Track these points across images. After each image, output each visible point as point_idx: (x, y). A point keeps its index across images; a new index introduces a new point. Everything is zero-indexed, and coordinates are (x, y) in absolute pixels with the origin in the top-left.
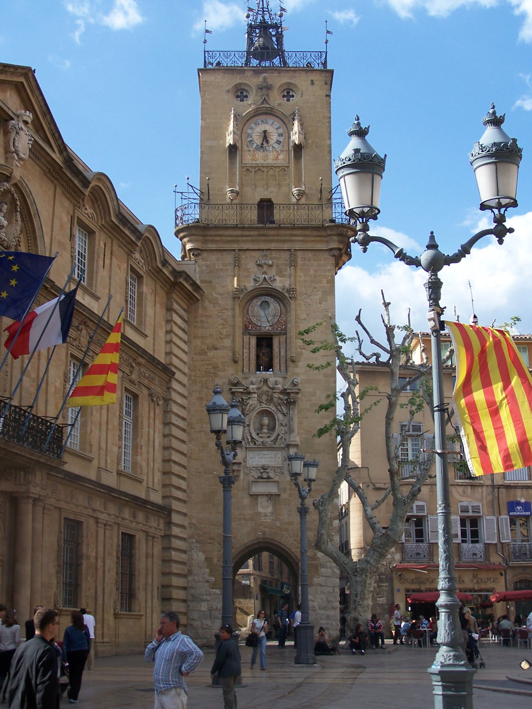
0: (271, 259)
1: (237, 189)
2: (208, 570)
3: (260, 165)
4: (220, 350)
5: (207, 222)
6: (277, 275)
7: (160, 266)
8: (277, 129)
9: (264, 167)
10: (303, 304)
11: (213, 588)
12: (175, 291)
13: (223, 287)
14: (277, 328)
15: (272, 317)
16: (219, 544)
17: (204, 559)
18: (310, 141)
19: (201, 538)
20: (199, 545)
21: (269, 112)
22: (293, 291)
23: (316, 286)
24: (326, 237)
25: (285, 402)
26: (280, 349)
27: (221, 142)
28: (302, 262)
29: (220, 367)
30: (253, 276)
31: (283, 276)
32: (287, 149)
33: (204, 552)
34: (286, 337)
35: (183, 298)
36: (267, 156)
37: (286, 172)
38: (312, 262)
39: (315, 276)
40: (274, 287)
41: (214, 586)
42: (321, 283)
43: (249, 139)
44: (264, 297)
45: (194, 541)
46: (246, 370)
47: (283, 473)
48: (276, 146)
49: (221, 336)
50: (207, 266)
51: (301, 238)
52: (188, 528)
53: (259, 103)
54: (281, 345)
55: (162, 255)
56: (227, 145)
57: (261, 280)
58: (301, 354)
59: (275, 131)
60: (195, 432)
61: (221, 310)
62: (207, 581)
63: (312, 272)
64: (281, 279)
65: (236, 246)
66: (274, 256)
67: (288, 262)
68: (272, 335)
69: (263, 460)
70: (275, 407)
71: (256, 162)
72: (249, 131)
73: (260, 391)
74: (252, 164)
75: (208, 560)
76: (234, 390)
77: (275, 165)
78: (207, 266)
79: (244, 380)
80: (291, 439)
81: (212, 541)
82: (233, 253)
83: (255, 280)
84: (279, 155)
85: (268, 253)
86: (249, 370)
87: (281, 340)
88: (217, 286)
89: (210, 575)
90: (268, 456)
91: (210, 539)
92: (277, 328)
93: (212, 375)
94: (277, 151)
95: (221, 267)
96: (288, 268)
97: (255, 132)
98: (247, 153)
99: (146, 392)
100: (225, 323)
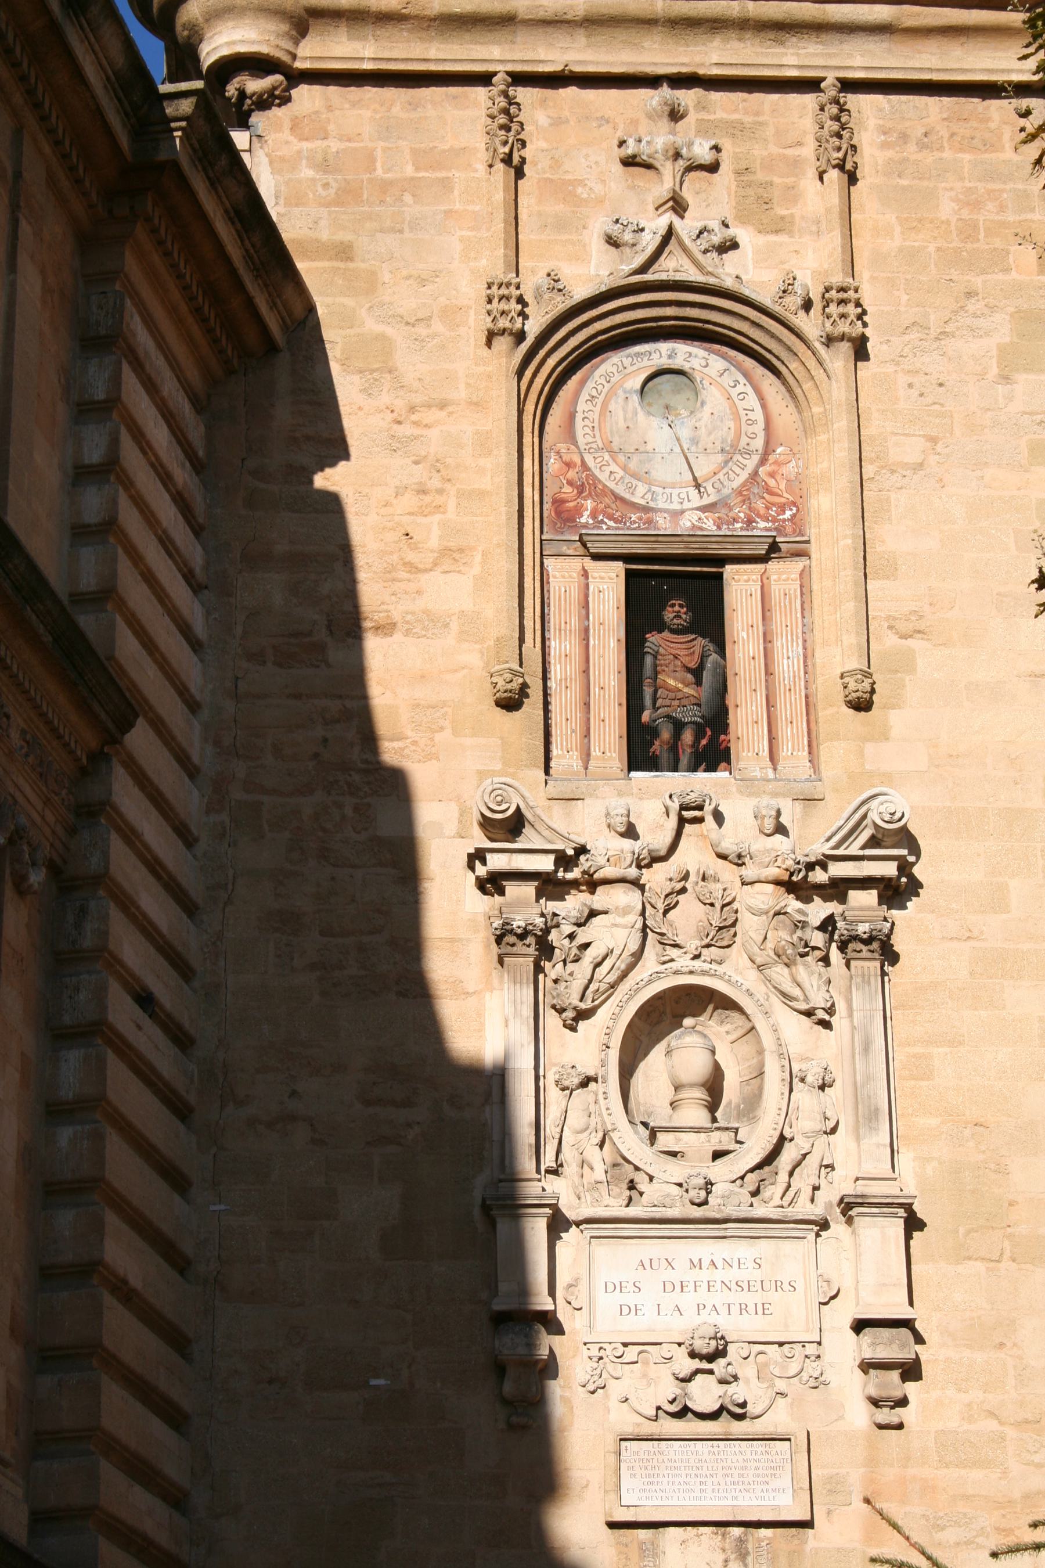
4: (407, 633)
6: (744, 219)
10: (902, 380)
13: (423, 282)
14: (750, 522)
15: (720, 458)
22: (842, 302)
23: (978, 282)
25: (818, 939)
26: (767, 639)
28: (890, 153)
29: (409, 733)
30: (600, 224)
31: (780, 227)
34: (805, 575)
35: (184, 308)
38: (947, 154)
39: (969, 231)
40: (729, 283)
42: (1007, 270)
44: (665, 347)
46: (564, 758)
47: (818, 1383)
49: (411, 556)
50: (325, 165)
54: (778, 618)
57: (649, 242)
58: (906, 663)
61: (412, 409)
63: (946, 209)
64: (762, 240)
66: (720, 115)
67: (808, 150)
68: (722, 561)
69: (688, 1300)
70: (753, 974)
73: (657, 877)
76: (497, 862)
78: (325, 165)
79: (557, 807)
80: (869, 1168)
82: (480, 93)
83: (613, 242)
85: (687, 97)
86: (586, 756)
87: (776, 589)
88: (387, 277)
90: (718, 1275)
92: (750, 522)
93: (356, 778)
95: (409, 171)
96: (809, 182)
100: (435, 483)
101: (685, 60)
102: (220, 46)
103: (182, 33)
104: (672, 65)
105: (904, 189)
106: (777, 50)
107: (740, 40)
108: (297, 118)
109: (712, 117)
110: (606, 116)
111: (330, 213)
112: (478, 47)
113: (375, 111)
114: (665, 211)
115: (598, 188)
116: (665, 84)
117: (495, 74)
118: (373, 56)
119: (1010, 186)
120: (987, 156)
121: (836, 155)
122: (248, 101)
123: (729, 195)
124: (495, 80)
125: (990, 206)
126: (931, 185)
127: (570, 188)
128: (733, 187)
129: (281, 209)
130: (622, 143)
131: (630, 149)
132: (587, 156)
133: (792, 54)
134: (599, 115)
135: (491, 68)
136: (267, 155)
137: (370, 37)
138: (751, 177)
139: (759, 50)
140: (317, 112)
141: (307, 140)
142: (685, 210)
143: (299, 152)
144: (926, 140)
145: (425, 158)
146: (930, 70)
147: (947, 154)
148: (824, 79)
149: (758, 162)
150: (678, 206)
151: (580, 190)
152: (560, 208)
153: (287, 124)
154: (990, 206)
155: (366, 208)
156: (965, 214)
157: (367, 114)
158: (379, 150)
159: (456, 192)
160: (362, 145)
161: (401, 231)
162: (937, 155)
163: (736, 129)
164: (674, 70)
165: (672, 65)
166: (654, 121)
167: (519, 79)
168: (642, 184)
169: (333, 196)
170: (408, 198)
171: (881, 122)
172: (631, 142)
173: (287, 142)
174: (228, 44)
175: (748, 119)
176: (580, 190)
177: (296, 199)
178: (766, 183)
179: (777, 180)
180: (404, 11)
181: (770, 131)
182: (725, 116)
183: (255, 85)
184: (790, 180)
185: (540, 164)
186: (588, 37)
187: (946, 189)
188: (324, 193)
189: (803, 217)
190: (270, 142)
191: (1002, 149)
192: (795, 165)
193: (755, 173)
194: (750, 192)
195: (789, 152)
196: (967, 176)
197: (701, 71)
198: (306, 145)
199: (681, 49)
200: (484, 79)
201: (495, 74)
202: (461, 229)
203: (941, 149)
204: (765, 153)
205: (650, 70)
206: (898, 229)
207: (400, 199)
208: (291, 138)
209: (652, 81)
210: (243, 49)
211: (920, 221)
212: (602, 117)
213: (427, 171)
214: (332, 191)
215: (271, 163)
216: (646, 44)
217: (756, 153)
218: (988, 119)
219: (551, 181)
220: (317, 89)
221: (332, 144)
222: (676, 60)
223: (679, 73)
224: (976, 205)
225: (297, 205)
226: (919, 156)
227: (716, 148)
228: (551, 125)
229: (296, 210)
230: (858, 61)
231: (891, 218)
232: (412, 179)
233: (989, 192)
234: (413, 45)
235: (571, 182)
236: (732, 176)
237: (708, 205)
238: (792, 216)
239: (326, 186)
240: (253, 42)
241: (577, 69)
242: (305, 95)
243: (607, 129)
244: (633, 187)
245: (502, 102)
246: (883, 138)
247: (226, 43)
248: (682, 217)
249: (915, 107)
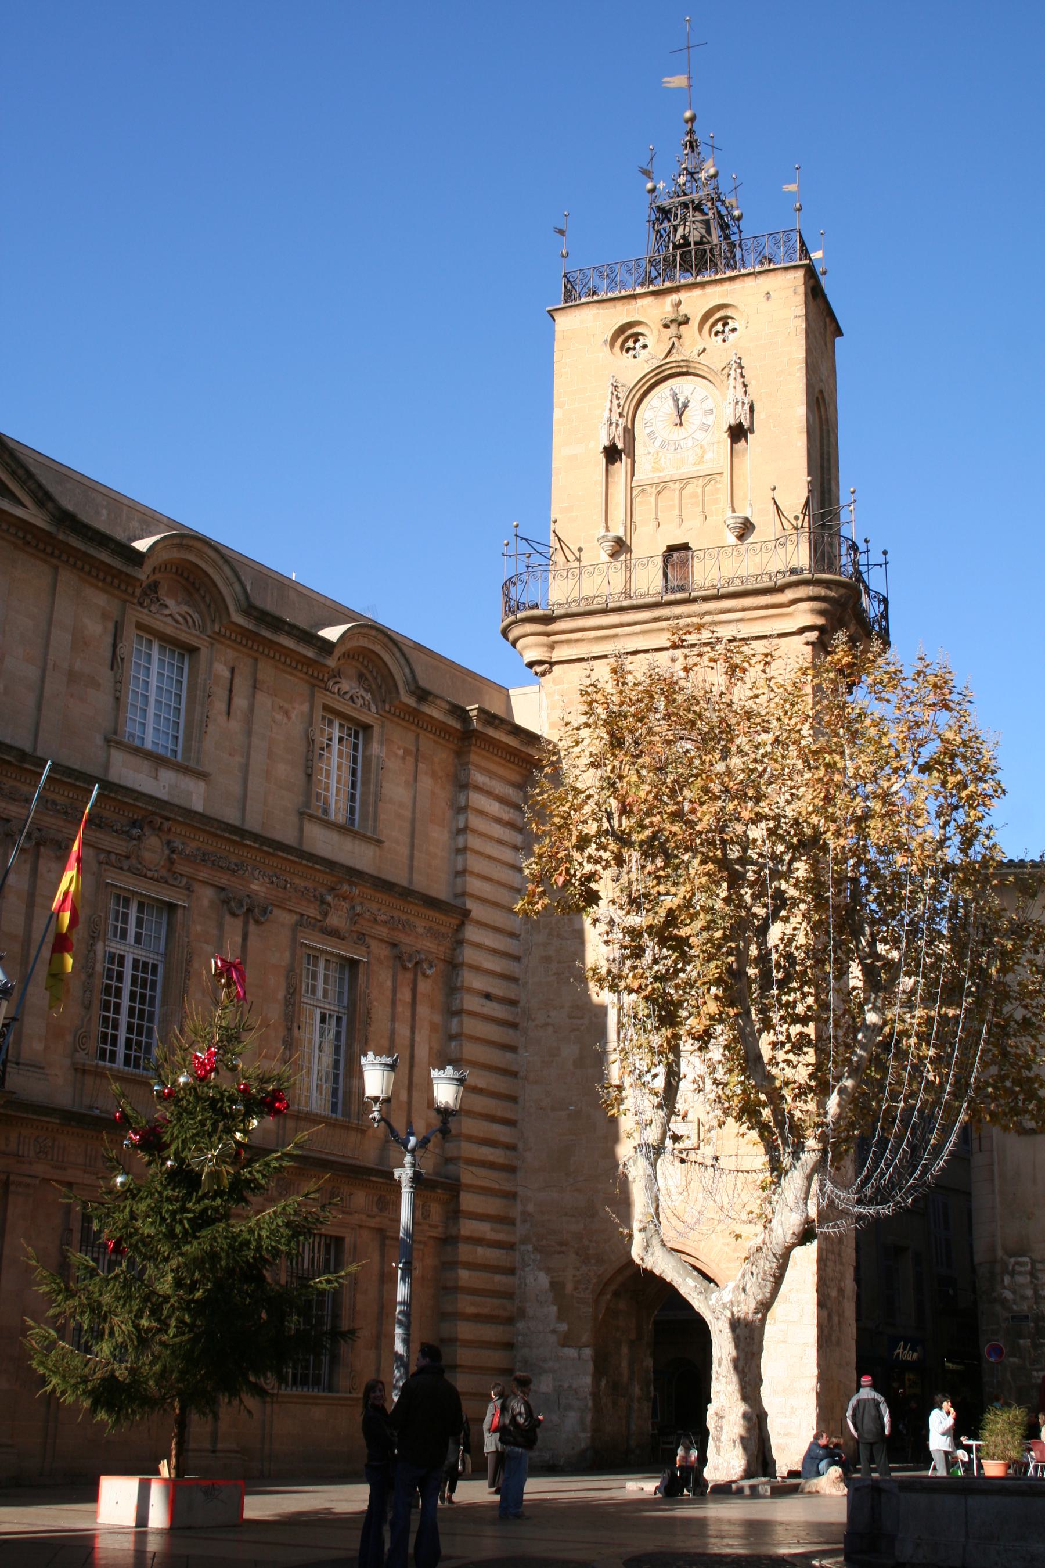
1: (618, 530)
2: (554, 1309)
7: (411, 701)
11: (564, 1346)
12: (473, 748)
16: (577, 1254)
17: (548, 1285)
19: (544, 1242)
20: (538, 1257)
21: (684, 370)
24: (788, 606)
33: (548, 1270)
41: (566, 1341)
43: (648, 430)
45: (530, 1247)
48: (700, 435)
52: (518, 1222)
55: (410, 680)
60: (536, 1026)
62: (554, 1331)
71: (661, 474)
74: (653, 478)
75: (556, 1286)
81: (564, 1248)
84: (704, 452)
89: (560, 1318)
91: (561, 1244)
94: (702, 447)
99: (381, 951)
220: (561, 666)
242: (556, 668)
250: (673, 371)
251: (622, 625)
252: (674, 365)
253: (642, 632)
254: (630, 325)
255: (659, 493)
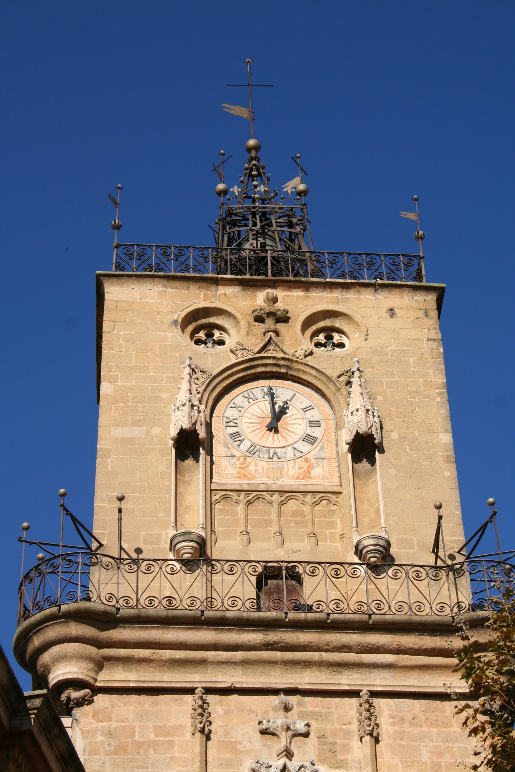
0: (301, 716)
3: (262, 487)
5: (114, 602)
6: (322, 761)
8: (305, 410)
9: (272, 492)
18: (395, 435)
21: (283, 370)
27: (156, 430)
28: (395, 728)
32: (335, 456)
36: (281, 469)
37: (333, 507)
38: (424, 729)
43: (231, 430)
48: (305, 447)
50: (109, 734)
51: (389, 658)
53: (257, 349)
56: (174, 432)
59: (299, 415)
63: (425, 756)
65: (197, 677)
66: (310, 708)
67: (354, 726)
71: (251, 482)
72: (231, 413)
74: (241, 484)
77: (302, 489)
78: (109, 734)
82: (189, 698)
84: (311, 466)
85: (293, 700)
94: (307, 460)
95: (152, 737)
96: (355, 743)
97: (246, 414)
98: (225, 462)
101: (292, 681)
102: (59, 675)
103: (40, 669)
104: (285, 683)
105: (403, 746)
106: (338, 677)
107: (319, 671)
108: (96, 711)
109: (305, 710)
110: (252, 709)
111: (111, 759)
112: (188, 675)
113: (136, 707)
114: (282, 757)
115: (248, 745)
116: (282, 693)
117: (196, 688)
118: (135, 680)
119: (457, 745)
120: (444, 729)
121: (368, 728)
122: (72, 703)
123: (315, 749)
124: (196, 691)
125: (447, 755)
126: (417, 744)
127: (234, 745)
128: (317, 745)
129: (86, 757)
130: (260, 723)
131: (264, 726)
132: (243, 729)
133: (345, 679)
134: (248, 708)
135: (195, 685)
136: (80, 729)
137: (134, 671)
138: (326, 740)
139: (329, 676)
140: (106, 708)
141: (101, 721)
142: (292, 756)
143: (97, 728)
144: (413, 721)
145: (160, 730)
146: (414, 686)
147: (424, 729)
148: (361, 691)
149: (329, 732)
150: (289, 754)
151: (239, 746)
152: (228, 755)
153: (91, 714)
154: (447, 755)
155: (130, 756)
156: (435, 759)
157: (132, 708)
158: (137, 726)
159: (176, 748)
160: (128, 724)
161: (147, 768)
162: (419, 729)
163: (318, 716)
164: (286, 686)
165: (285, 683)
166: (276, 711)
167: (209, 691)
168: (270, 743)
169: (113, 750)
170: (151, 751)
171: (391, 712)
172: (265, 722)
173: (90, 723)
174: (63, 674)
175: (323, 711)
176: (239, 746)
177: (93, 752)
178: (333, 743)
179: (339, 741)
180: (151, 657)
181: (335, 717)
182: (312, 709)
183: (75, 694)
184: (345, 741)
185: (219, 733)
186: (243, 670)
187: (424, 746)
188: (108, 749)
189: (352, 760)
190: (82, 723)
191: (452, 726)
192: (348, 733)
193: (327, 738)
194: (325, 747)
195: (345, 727)
196: (435, 739)
197: (300, 687)
198: (100, 724)
199: (290, 676)
200: (191, 691)
201: (196, 688)
202: (178, 767)
203: (421, 726)
204: (333, 728)
205: (274, 686)
206: (401, 767)
207: (147, 751)
208: (93, 721)
209: (275, 692)
210: (70, 676)
211: (412, 762)
212: (250, 710)
213: (161, 737)
214: (113, 747)
215: (82, 733)
216: (273, 673)
217: (328, 727)
218: (444, 711)
219: (224, 741)
220: (107, 696)
221: (113, 724)
222: (287, 682)
223: (289, 688)
224: (440, 754)
225: (94, 755)
226: (410, 729)
227: (308, 725)
228: (224, 714)
229: (94, 757)
230: (378, 682)
231: (397, 760)
232: (154, 741)
233: (447, 748)
234: (155, 674)
235: (234, 742)
236: (316, 739)
237: (304, 754)
238: (347, 759)
239: (110, 745)
240: (75, 673)
241: (238, 686)
242: (101, 699)
243: (253, 716)
244: (265, 745)
245: (200, 702)
246: (392, 720)
247: (62, 673)
248: (291, 760)
249: (407, 705)
250: (268, 369)
251: (215, 647)
252: (271, 361)
253: (244, 663)
254: (207, 312)
255: (249, 503)
